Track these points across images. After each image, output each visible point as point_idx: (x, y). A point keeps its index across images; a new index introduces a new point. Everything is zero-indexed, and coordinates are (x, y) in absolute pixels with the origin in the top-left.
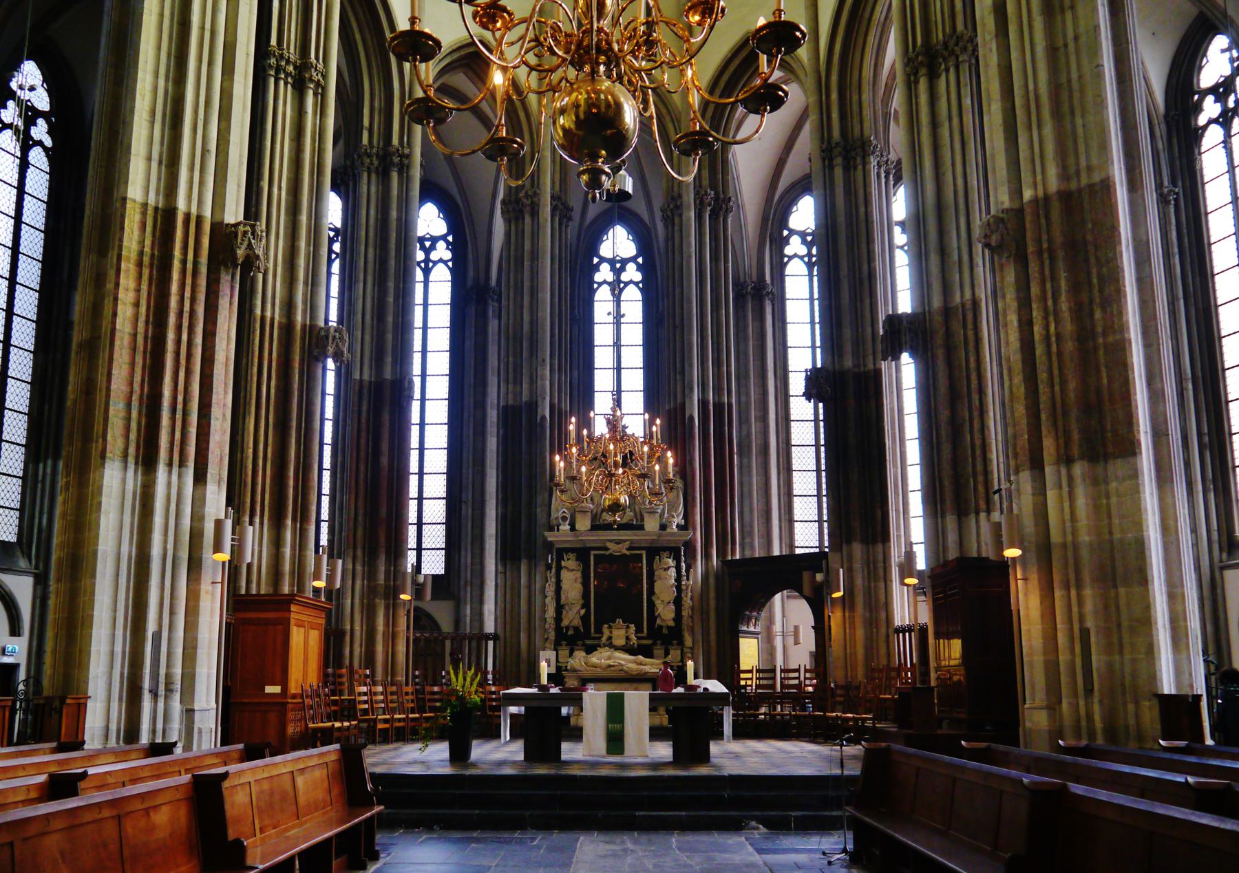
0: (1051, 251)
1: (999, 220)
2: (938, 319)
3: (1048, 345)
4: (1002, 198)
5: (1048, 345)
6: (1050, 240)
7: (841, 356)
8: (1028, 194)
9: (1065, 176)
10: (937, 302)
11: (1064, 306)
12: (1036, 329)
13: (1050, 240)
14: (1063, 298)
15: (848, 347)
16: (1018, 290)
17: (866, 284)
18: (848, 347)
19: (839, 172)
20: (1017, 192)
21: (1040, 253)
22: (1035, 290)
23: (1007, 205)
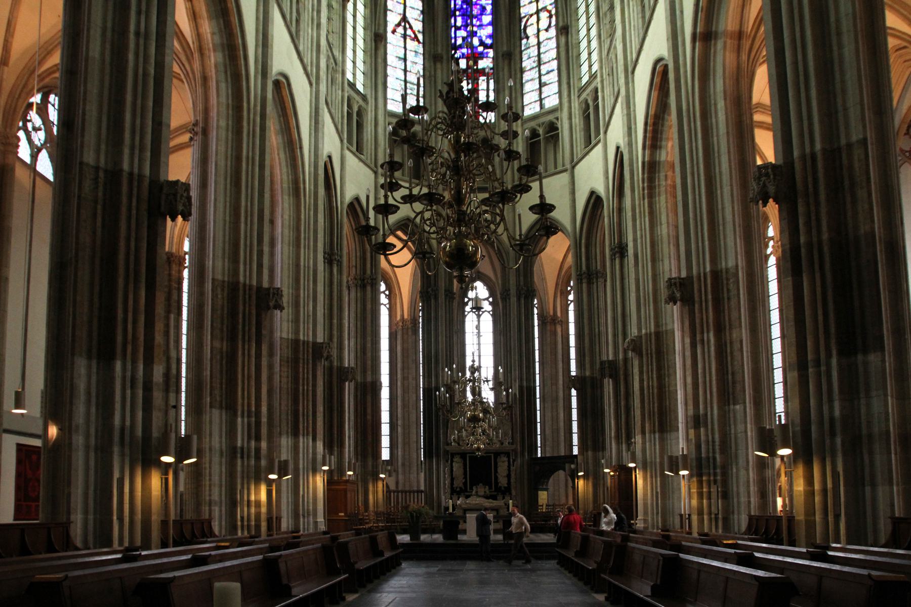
0: (651, 354)
1: (632, 340)
2: (621, 363)
3: (649, 389)
4: (633, 331)
5: (649, 389)
6: (651, 350)
7: (585, 370)
8: (644, 331)
9: (657, 325)
10: (621, 357)
11: (655, 376)
12: (645, 383)
13: (651, 350)
14: (655, 372)
15: (588, 366)
16: (639, 368)
17: (597, 337)
18: (588, 366)
19: (585, 286)
20: (640, 329)
21: (647, 354)
22: (645, 369)
23: (636, 334)
